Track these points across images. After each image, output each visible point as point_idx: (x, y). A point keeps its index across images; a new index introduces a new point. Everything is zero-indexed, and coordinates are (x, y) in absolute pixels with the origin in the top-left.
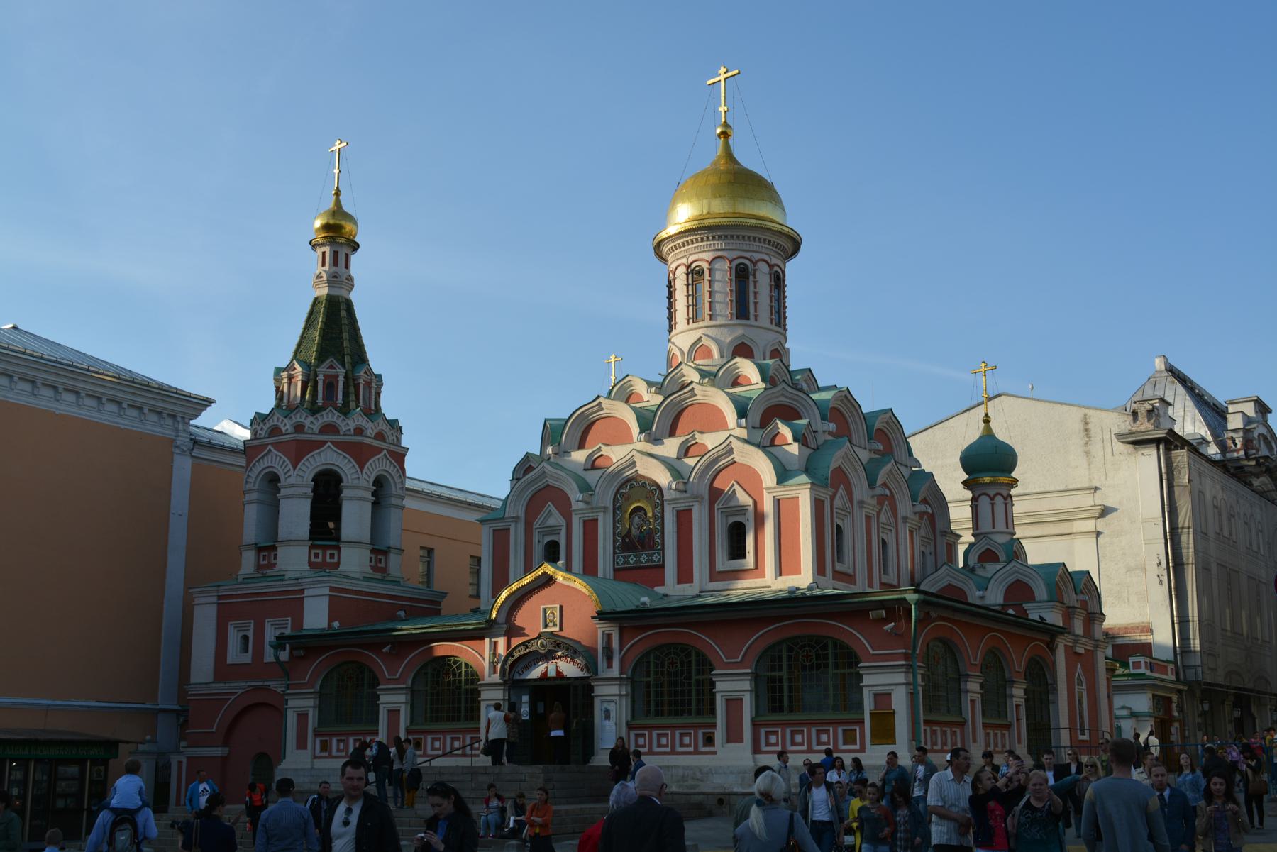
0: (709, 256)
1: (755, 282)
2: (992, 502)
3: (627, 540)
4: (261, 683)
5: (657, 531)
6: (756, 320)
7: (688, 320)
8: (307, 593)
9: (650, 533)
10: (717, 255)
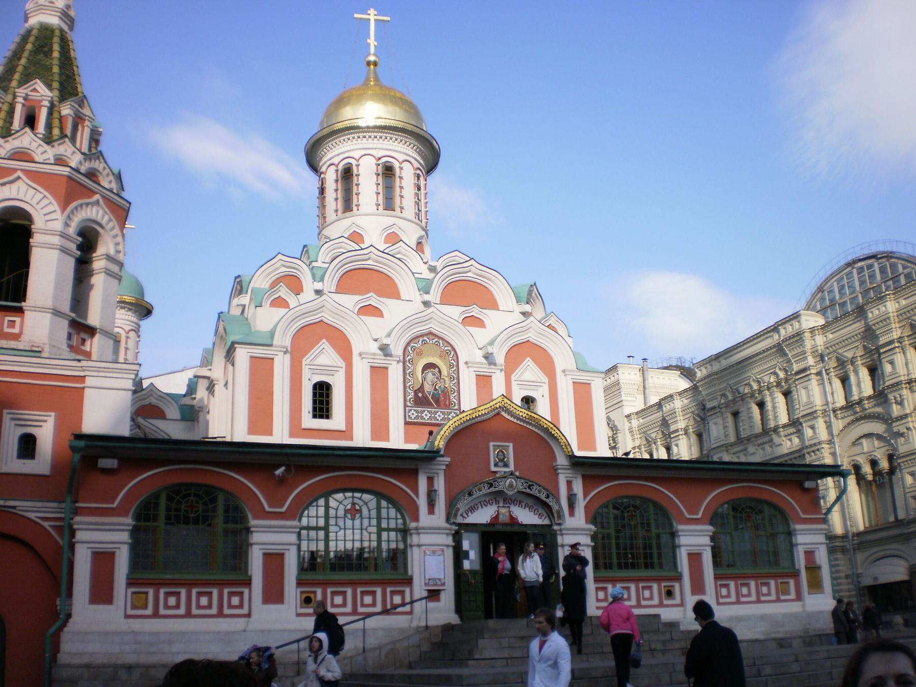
0: (401, 157)
3: (420, 395)
7: (378, 205)
8: (89, 382)
9: (446, 393)
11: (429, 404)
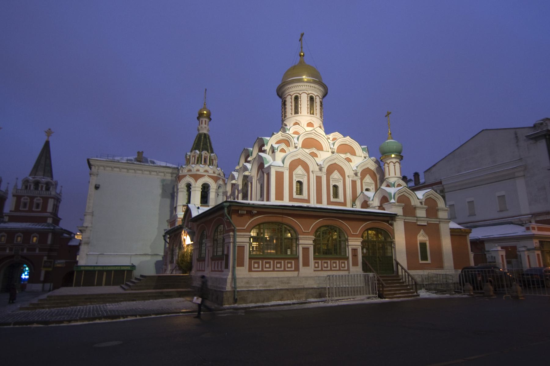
1: (300, 101)
2: (395, 165)
6: (301, 113)
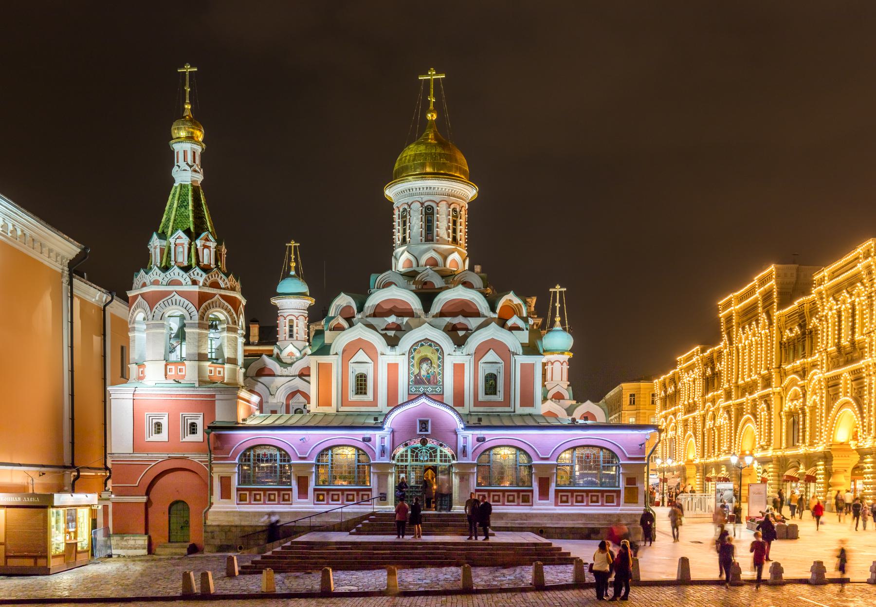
3: (418, 378)
4: (182, 455)
5: (439, 374)
8: (217, 397)
10: (442, 199)
11: (424, 383)
